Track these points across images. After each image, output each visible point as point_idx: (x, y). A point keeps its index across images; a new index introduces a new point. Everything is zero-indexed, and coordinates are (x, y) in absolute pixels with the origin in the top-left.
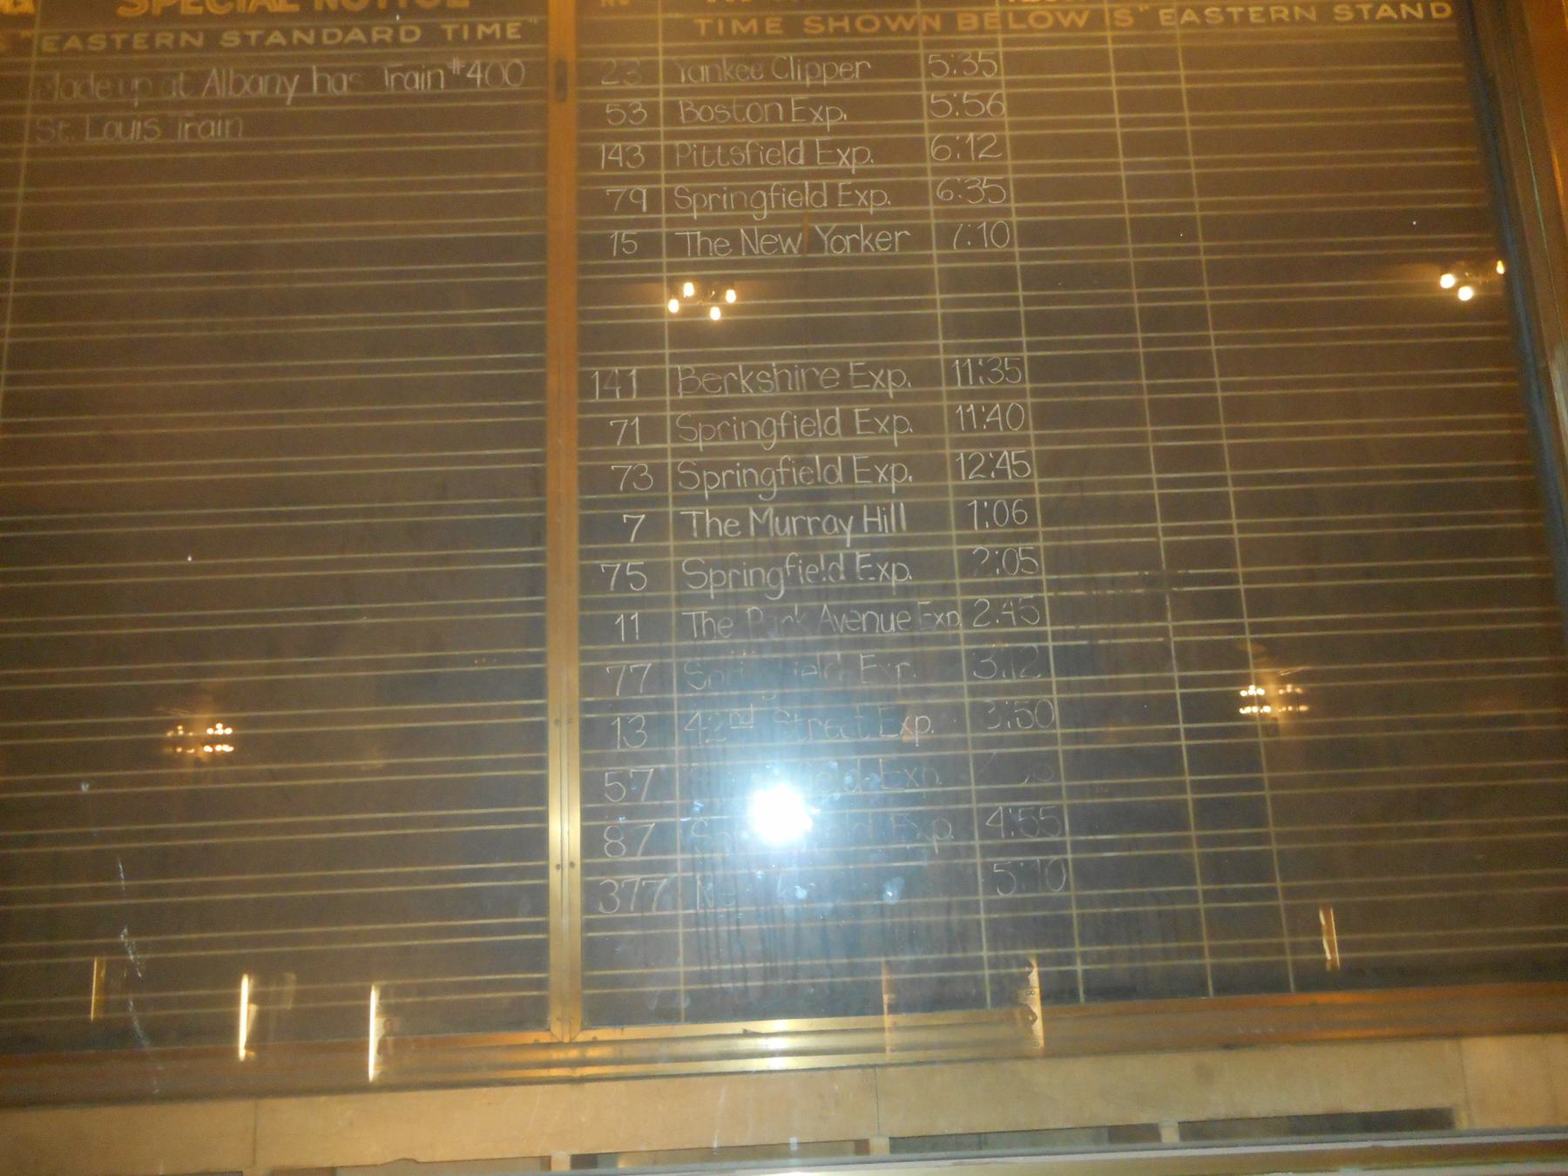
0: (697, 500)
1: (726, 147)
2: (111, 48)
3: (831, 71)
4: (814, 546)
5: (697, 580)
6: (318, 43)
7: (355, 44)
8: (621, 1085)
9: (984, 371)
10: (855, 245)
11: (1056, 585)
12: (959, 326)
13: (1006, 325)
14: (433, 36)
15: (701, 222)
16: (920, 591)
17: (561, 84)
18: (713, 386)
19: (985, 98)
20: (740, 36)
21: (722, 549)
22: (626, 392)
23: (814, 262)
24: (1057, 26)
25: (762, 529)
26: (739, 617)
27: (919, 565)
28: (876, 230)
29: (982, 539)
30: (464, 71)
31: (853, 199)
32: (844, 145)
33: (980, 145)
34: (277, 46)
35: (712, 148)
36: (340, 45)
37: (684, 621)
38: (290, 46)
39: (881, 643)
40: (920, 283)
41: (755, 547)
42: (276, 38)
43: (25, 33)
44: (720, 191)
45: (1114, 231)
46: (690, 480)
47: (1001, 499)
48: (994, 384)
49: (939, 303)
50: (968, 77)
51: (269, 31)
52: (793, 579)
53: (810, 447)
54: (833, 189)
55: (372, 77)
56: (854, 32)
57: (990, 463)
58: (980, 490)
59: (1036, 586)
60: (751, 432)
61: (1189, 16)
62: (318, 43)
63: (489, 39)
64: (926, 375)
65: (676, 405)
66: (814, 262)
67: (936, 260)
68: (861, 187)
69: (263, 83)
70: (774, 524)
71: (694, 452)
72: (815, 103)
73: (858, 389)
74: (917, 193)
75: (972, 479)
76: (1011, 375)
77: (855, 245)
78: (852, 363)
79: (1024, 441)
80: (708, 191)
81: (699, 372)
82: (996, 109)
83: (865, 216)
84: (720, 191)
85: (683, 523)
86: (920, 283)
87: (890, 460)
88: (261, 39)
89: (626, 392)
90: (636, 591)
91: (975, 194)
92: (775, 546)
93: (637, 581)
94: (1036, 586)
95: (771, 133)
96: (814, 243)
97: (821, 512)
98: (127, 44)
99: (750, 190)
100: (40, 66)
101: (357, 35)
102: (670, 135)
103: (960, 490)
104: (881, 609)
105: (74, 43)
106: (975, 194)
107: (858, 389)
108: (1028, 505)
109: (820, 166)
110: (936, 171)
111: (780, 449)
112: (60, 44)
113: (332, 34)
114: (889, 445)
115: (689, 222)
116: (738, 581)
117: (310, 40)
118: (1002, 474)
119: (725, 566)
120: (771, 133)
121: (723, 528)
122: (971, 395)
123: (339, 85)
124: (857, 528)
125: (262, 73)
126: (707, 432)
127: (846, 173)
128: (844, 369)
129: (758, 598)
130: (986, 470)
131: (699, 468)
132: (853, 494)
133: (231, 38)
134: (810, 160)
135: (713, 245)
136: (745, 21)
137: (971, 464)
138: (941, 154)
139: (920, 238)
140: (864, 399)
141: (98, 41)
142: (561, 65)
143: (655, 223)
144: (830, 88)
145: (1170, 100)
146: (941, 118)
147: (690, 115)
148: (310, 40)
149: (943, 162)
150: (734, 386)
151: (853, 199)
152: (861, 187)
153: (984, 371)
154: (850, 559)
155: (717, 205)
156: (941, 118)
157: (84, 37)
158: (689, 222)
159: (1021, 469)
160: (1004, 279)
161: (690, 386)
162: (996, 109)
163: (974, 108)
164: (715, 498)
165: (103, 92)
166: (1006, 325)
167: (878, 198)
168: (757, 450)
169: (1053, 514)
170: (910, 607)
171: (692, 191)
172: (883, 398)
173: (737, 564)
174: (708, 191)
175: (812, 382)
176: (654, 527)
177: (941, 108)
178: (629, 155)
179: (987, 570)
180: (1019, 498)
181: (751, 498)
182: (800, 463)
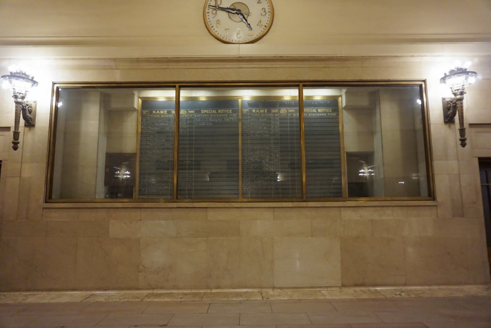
12: (274, 143)
13: (278, 143)
14: (229, 115)
27: (269, 164)
45: (288, 135)
49: (272, 141)
55: (223, 119)
67: (272, 137)
74: (271, 131)
86: (270, 139)
113: (220, 115)
145: (293, 123)
160: (278, 139)
166: (278, 143)
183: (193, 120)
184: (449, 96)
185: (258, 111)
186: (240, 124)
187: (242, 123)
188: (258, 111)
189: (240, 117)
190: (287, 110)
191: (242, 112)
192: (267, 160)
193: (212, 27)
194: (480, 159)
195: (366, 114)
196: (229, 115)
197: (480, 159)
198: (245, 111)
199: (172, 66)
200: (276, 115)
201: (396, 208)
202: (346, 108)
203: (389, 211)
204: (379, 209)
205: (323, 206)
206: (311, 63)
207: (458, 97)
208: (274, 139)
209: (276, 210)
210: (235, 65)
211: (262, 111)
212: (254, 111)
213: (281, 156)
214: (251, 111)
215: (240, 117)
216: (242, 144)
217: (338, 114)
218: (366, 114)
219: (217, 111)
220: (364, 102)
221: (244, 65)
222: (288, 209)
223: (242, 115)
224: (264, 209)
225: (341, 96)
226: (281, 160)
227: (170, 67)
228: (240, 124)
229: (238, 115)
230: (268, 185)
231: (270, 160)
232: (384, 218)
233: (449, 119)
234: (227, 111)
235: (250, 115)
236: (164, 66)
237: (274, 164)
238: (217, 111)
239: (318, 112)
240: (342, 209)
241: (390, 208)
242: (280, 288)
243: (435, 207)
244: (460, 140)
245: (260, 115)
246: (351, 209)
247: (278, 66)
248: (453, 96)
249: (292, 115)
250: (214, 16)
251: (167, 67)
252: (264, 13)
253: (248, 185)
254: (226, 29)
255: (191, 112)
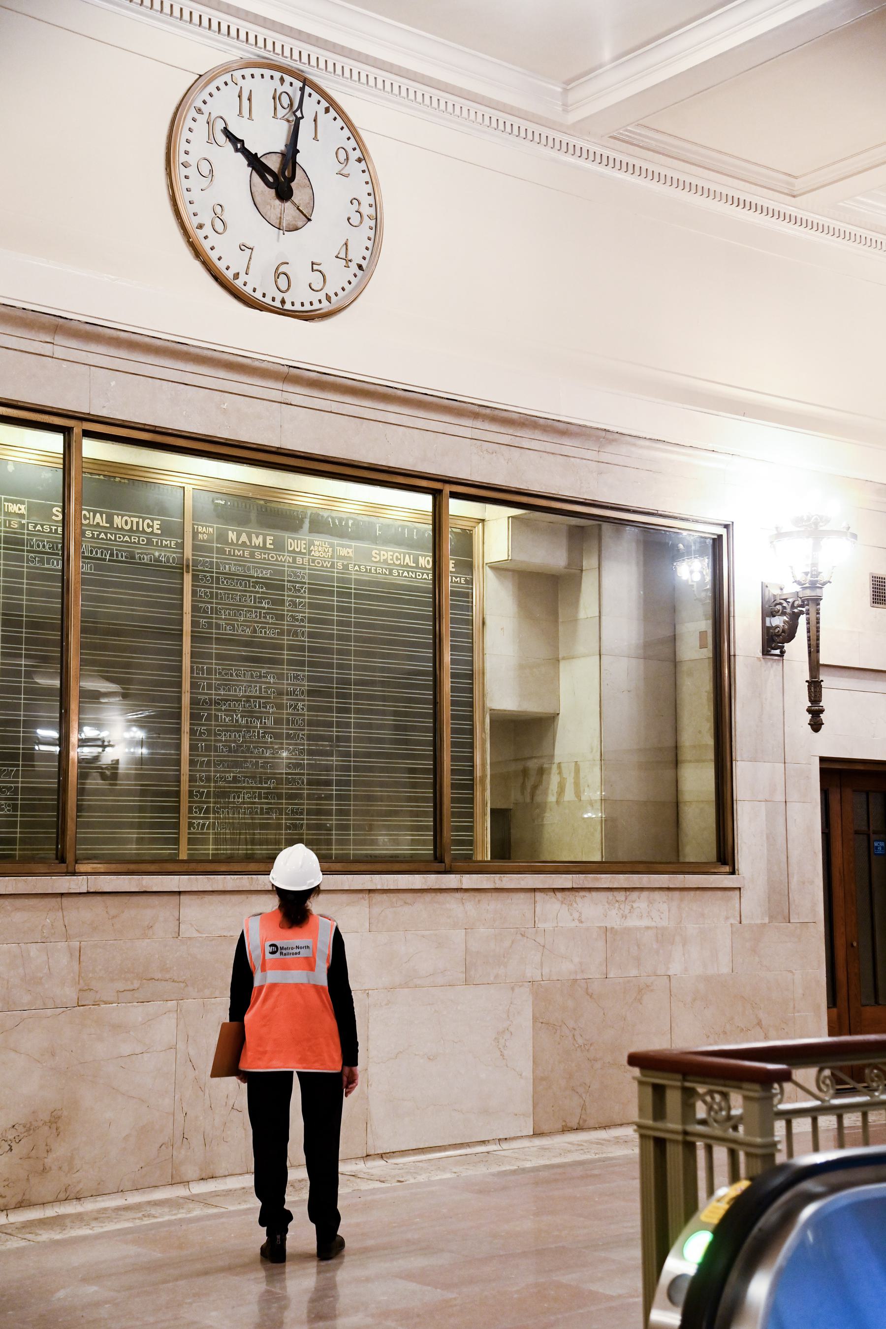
0: (221, 710)
1: (233, 594)
2: (51, 532)
3: (262, 572)
4: (250, 727)
5: (220, 735)
6: (115, 540)
7: (126, 542)
8: (155, 890)
9: (296, 677)
10: (265, 632)
11: (309, 745)
12: (291, 662)
13: (302, 663)
14: (149, 542)
15: (225, 619)
16: (276, 744)
17: (188, 566)
18: (226, 674)
19: (302, 588)
20: (237, 556)
21: (226, 726)
22: (203, 674)
23: (254, 637)
24: (322, 566)
25: (237, 721)
26: (230, 747)
28: (271, 628)
29: (292, 729)
30: (159, 557)
31: (265, 617)
32: (265, 598)
33: (300, 603)
34: (102, 539)
35: (229, 594)
36: (122, 541)
37: (216, 747)
38: (107, 540)
39: (265, 758)
40: (281, 647)
41: (234, 726)
42: (102, 536)
43: (23, 522)
44: (230, 609)
46: (219, 704)
47: (297, 718)
48: (298, 682)
49: (286, 655)
50: (298, 580)
51: (100, 533)
52: (244, 737)
53: (250, 697)
54: (260, 613)
56: (269, 560)
57: (296, 706)
58: (293, 714)
59: (303, 745)
60: (235, 691)
61: (357, 568)
62: (115, 540)
63: (166, 546)
64: (280, 676)
65: (216, 679)
66: (254, 637)
67: (286, 640)
68: (268, 613)
69: (99, 551)
70: (240, 720)
71: (220, 695)
72: (257, 583)
73: (263, 680)
75: (290, 711)
76: (303, 680)
77: (265, 632)
78: (264, 671)
79: (303, 700)
80: (227, 609)
81: (223, 669)
82: (305, 592)
83: (268, 623)
84: (230, 609)
85: (216, 716)
87: (271, 703)
88: (98, 535)
89: (203, 674)
90: (204, 737)
91: (297, 620)
92: (240, 726)
93: (204, 734)
94: (303, 745)
95: (245, 591)
96: (255, 631)
97: (252, 717)
98: (56, 530)
99: (238, 610)
100: (28, 534)
101: (127, 538)
102: (217, 588)
103: (288, 714)
104: (265, 748)
105: (39, 527)
106: (297, 620)
107: (263, 680)
108: (303, 720)
109: (257, 605)
110: (288, 611)
111: (243, 696)
112: (35, 527)
114: (270, 698)
115: (221, 619)
116: (230, 736)
117: (113, 538)
118: (298, 710)
119: (227, 731)
120: (245, 591)
121: (227, 720)
122: (293, 685)
123: (122, 557)
124: (261, 723)
125: (99, 548)
126: (224, 689)
127: (264, 608)
128: (260, 672)
129: (235, 742)
130: (294, 709)
131: (222, 700)
132: (261, 712)
133: (88, 534)
134: (255, 603)
135: (228, 628)
136: (239, 551)
137: (291, 706)
138: (290, 605)
139: (281, 633)
140: (266, 683)
141: (47, 528)
142: (188, 560)
143: (212, 618)
144: (262, 578)
146: (290, 593)
147: (223, 582)
148: (113, 538)
149: (290, 608)
150: (232, 675)
151: (265, 617)
152: (268, 613)
153: (296, 677)
154: (259, 732)
155: (229, 614)
156: (290, 593)
157: (42, 526)
158: (221, 619)
159: (303, 709)
160: (302, 648)
161: (220, 673)
162: (305, 592)
163: (299, 591)
164: (225, 710)
165: (50, 548)
166: (302, 663)
167: (272, 618)
168: (236, 696)
169: (310, 723)
170: (273, 748)
171: (223, 608)
172: (270, 683)
173: (230, 731)
174: (227, 609)
175: (252, 676)
176: (209, 718)
177: (290, 590)
178: (206, 593)
179: (292, 739)
180: (302, 718)
181: (234, 711)
182: (248, 701)
183: (21, 542)
184: (788, 587)
185: (244, 538)
186: (188, 579)
187: (195, 578)
188: (244, 538)
189: (188, 552)
190: (332, 545)
191: (195, 534)
192: (270, 723)
193: (200, 226)
194: (822, 760)
195: (547, 593)
196: (149, 542)
197: (822, 760)
198: (207, 531)
199: (65, 347)
200: (299, 560)
201: (657, 895)
202: (497, 568)
203: (641, 902)
204: (621, 896)
205: (499, 885)
206: (478, 424)
207: (808, 593)
208: (291, 648)
209: (377, 897)
210: (272, 390)
211: (258, 541)
212: (232, 536)
213: (310, 708)
214: (222, 537)
215: (188, 552)
216: (193, 655)
217: (470, 582)
218: (547, 593)
219: (110, 520)
220: (550, 555)
221: (297, 394)
222: (409, 897)
223: (195, 548)
224: (344, 897)
225: (483, 520)
226: (310, 723)
227: (59, 352)
228: (188, 579)
229: (181, 546)
230: (269, 811)
231: (278, 721)
232: (633, 922)
233: (774, 642)
234: (144, 525)
235: (221, 551)
236: (36, 342)
237: (288, 736)
238: (110, 520)
239: (417, 567)
240: (539, 895)
241: (645, 894)
242: (382, 1156)
243: (737, 892)
244: (809, 711)
245: (252, 555)
246: (559, 895)
247: (392, 418)
248: (798, 588)
249: (346, 567)
250: (205, 182)
251: (47, 349)
252: (355, 219)
253: (207, 811)
254: (243, 247)
255: (14, 508)
